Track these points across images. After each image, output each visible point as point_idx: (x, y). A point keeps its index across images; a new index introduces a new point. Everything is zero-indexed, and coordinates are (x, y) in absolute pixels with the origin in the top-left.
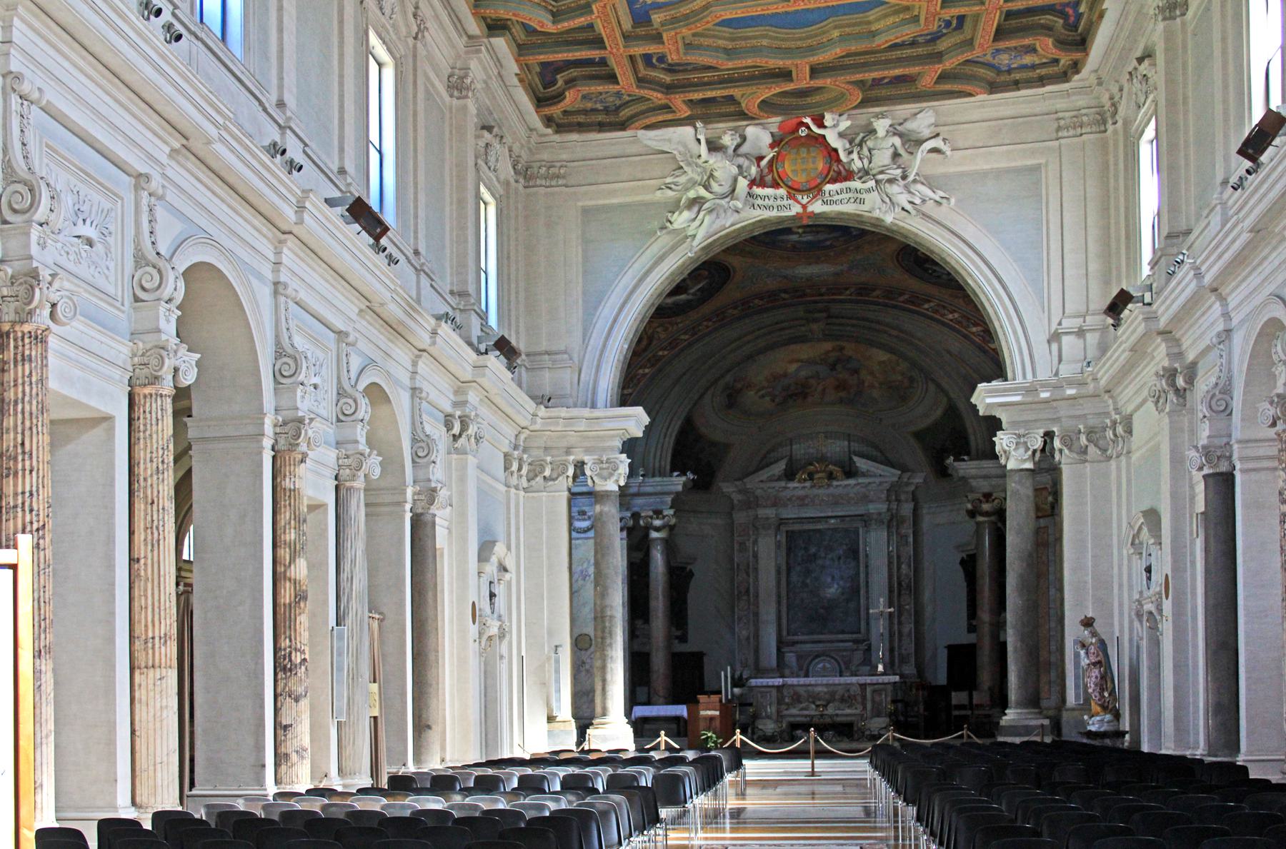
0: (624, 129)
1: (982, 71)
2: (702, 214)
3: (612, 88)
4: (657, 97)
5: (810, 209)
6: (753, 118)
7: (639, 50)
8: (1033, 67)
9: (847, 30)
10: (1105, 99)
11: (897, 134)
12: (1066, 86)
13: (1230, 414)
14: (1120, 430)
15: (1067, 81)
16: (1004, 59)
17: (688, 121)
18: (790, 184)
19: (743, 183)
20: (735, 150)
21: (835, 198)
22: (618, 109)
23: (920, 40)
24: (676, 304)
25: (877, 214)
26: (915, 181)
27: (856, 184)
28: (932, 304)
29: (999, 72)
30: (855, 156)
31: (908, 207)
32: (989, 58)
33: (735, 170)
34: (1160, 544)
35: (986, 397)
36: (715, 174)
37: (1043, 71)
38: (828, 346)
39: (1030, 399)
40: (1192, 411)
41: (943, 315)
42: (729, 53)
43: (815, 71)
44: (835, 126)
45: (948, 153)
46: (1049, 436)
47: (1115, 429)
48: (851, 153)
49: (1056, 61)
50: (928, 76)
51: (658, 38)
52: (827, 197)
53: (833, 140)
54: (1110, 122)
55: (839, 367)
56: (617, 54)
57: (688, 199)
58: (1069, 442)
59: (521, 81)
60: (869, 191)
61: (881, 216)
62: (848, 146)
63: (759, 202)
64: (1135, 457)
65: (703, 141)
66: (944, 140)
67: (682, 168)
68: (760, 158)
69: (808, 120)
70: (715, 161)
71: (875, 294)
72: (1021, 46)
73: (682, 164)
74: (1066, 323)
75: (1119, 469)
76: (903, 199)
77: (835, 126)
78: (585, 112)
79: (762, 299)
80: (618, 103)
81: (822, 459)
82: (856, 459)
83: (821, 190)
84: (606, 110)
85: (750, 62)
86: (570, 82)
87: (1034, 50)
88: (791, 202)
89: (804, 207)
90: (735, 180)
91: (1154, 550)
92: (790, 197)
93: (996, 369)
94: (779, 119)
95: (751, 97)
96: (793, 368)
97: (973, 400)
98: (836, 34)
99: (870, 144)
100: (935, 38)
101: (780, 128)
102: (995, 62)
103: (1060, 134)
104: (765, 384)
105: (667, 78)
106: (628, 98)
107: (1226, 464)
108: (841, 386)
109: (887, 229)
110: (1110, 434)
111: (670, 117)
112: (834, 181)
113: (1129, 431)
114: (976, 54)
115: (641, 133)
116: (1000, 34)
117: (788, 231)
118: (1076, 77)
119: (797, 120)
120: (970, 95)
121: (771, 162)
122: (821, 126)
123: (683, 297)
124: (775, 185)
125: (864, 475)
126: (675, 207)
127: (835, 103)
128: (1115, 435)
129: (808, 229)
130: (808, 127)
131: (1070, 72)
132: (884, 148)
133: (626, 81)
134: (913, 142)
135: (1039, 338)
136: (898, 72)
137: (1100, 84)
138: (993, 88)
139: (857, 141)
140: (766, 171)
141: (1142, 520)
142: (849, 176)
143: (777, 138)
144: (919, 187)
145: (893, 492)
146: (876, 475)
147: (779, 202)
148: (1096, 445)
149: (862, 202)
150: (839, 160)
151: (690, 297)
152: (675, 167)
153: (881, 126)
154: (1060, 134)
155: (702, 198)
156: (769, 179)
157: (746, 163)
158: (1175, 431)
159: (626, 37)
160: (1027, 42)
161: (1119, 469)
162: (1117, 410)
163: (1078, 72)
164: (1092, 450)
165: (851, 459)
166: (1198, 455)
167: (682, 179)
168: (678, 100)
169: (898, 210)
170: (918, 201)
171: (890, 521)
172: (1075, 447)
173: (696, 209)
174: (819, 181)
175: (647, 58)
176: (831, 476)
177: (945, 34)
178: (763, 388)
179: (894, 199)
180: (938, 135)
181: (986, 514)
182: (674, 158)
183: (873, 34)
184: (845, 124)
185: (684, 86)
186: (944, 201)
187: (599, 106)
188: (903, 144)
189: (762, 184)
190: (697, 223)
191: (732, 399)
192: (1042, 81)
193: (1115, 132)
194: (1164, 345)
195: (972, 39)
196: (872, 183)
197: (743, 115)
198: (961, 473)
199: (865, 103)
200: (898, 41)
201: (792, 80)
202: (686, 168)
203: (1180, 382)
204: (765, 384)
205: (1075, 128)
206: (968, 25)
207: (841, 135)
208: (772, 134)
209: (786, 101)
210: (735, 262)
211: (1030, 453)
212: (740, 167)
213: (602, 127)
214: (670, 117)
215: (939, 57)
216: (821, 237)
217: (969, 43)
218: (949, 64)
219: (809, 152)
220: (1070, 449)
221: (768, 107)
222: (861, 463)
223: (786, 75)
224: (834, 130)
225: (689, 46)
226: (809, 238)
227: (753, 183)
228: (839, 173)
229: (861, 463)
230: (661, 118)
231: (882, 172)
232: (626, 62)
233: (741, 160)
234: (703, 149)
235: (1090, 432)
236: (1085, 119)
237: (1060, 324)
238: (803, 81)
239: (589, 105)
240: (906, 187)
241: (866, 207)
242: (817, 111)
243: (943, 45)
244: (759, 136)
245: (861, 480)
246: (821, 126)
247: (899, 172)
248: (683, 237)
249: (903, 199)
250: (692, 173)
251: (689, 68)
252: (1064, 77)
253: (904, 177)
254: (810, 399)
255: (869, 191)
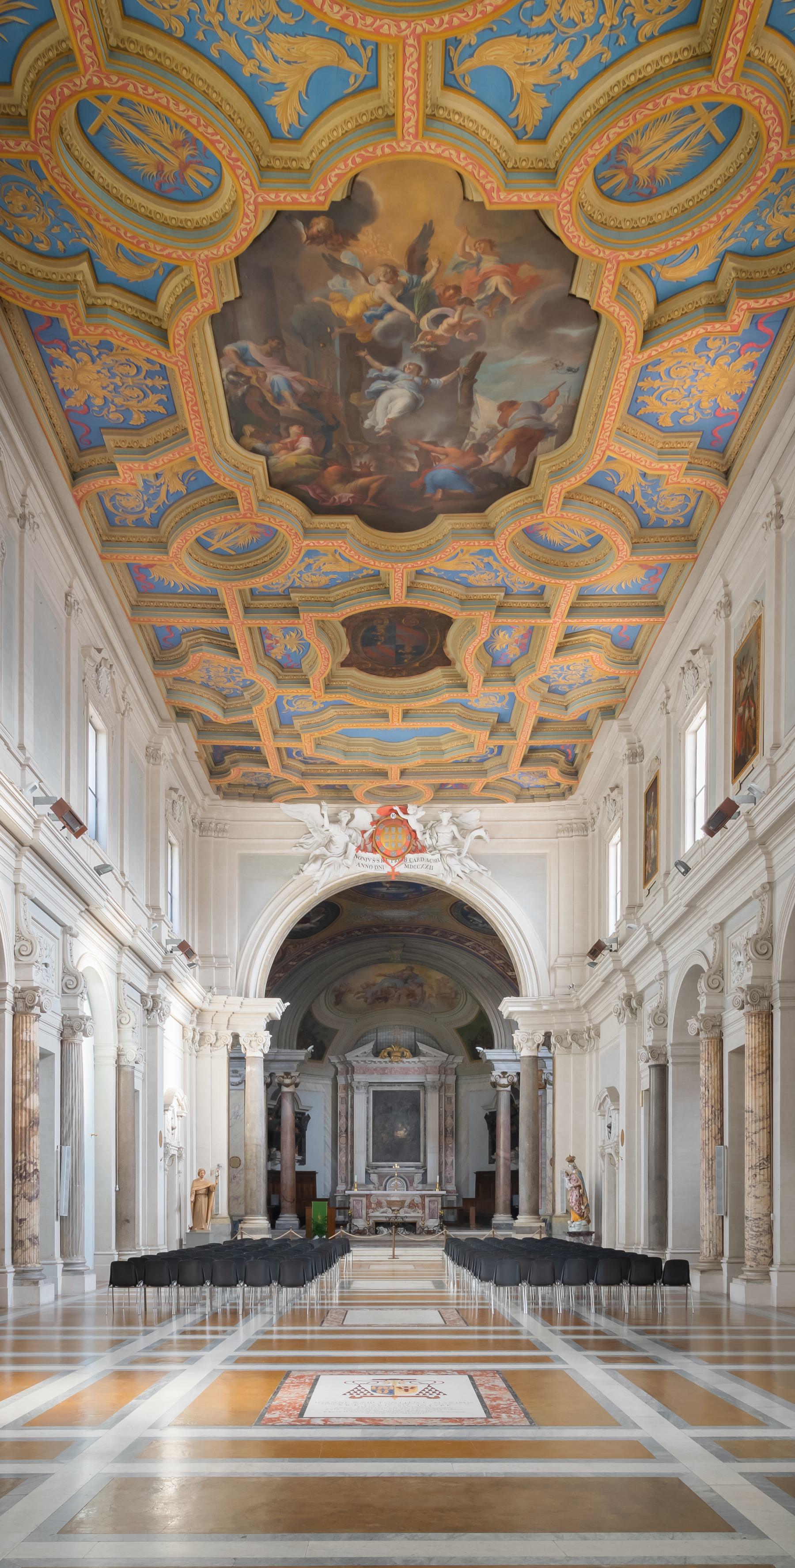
0: (271, 801)
1: (511, 786)
2: (324, 866)
3: (263, 770)
4: (295, 780)
5: (397, 870)
6: (360, 803)
7: (284, 744)
8: (544, 787)
9: (427, 747)
10: (588, 814)
11: (455, 823)
12: (564, 802)
13: (666, 1026)
14: (592, 1033)
15: (565, 799)
16: (526, 780)
17: (316, 800)
18: (384, 851)
19: (352, 848)
20: (347, 824)
21: (414, 864)
22: (267, 786)
23: (473, 760)
24: (302, 930)
25: (441, 877)
26: (466, 857)
27: (427, 855)
28: (471, 943)
29: (522, 788)
30: (427, 836)
31: (461, 874)
32: (516, 778)
33: (348, 839)
34: (618, 1109)
35: (509, 1006)
36: (333, 839)
37: (550, 791)
38: (402, 966)
39: (535, 1009)
40: (640, 1023)
41: (478, 951)
42: (345, 753)
43: (403, 773)
44: (415, 814)
45: (488, 840)
46: (548, 1036)
47: (589, 1034)
48: (424, 834)
49: (558, 785)
50: (478, 784)
51: (298, 737)
52: (408, 863)
53: (414, 825)
54: (590, 829)
55: (409, 981)
56: (268, 745)
57: (314, 856)
58: (560, 1040)
59: (199, 757)
60: (436, 861)
61: (444, 879)
62: (422, 828)
63: (362, 862)
64: (601, 1052)
65: (326, 816)
66: (485, 831)
67: (310, 833)
68: (364, 832)
69: (396, 808)
70: (334, 829)
71: (435, 933)
72: (538, 772)
73: (311, 830)
74: (559, 960)
75: (591, 1059)
76: (457, 869)
77: (415, 814)
78: (244, 786)
79: (359, 930)
80: (267, 781)
81: (397, 1043)
82: (419, 1044)
83: (404, 858)
84: (259, 786)
85: (360, 762)
86: (235, 762)
87: (546, 776)
88: (384, 864)
89: (393, 868)
90: (347, 845)
91: (614, 1114)
92: (384, 860)
93: (513, 987)
94: (379, 805)
95: (361, 786)
96: (379, 980)
97: (500, 1008)
98: (418, 749)
99: (438, 829)
100: (482, 761)
101: (378, 812)
102: (520, 781)
103: (559, 835)
104: (361, 989)
105: (303, 767)
106: (274, 779)
107: (663, 1059)
108: (411, 995)
109: (447, 888)
110: (586, 1036)
111: (303, 795)
112: (413, 852)
113: (598, 1035)
114: (508, 774)
115: (283, 805)
116: (525, 760)
117: (379, 884)
118: (571, 797)
119: (389, 808)
120: (503, 802)
121: (372, 837)
122: (405, 813)
123: (308, 925)
124: (374, 851)
125: (424, 1055)
126: (305, 860)
127: (415, 797)
128: (589, 1037)
129: (393, 885)
130: (397, 813)
131: (567, 793)
132: (445, 834)
133: (274, 768)
134: (464, 831)
135: (542, 968)
136: (457, 780)
137: (585, 803)
138: (518, 798)
139: (429, 826)
140: (367, 841)
141: (606, 1093)
142: (423, 849)
143: (376, 819)
144: (468, 861)
145: (442, 1070)
146: (432, 1056)
147: (376, 863)
148: (577, 1043)
149: (431, 868)
150: (416, 838)
151: (312, 925)
152: (305, 832)
153: (445, 817)
154: (559, 835)
155: (325, 855)
156: (369, 847)
157: (354, 835)
158: (630, 1036)
159: (275, 733)
160: (542, 769)
161: (591, 1059)
162: (590, 1020)
163: (572, 794)
164: (574, 1045)
165: (416, 1045)
166: (644, 1051)
167: (310, 841)
168: (310, 786)
169: (454, 876)
170: (467, 871)
171: (440, 1088)
172: (564, 1043)
173: (319, 862)
174: (403, 851)
175: (289, 751)
176: (403, 1056)
177: (489, 758)
178: (359, 993)
179: (453, 869)
180: (481, 827)
181: (504, 1086)
182: (305, 825)
183: (443, 752)
184: (421, 813)
185: (313, 775)
186: (484, 873)
187: (254, 783)
188: (459, 831)
189: (365, 850)
190: (320, 873)
191: (339, 998)
192: (549, 797)
193: (593, 836)
194: (624, 979)
195: (507, 763)
196: (438, 856)
197: (353, 800)
198: (488, 1058)
199: (435, 800)
200: (459, 759)
201: (388, 779)
202: (314, 834)
203: (634, 1003)
204: (361, 989)
205: (568, 831)
206: (505, 751)
207: (419, 821)
208: (373, 816)
209: (382, 793)
210: (344, 904)
211: (536, 1045)
212: (350, 836)
213: (255, 798)
214: (303, 795)
215: (484, 773)
216: (402, 891)
217: (505, 766)
218: (492, 778)
219: (397, 830)
220: (561, 1045)
221: (371, 795)
222: (423, 1047)
223: (384, 774)
224: (414, 816)
225: (318, 745)
226: (393, 891)
227: (359, 848)
228: (417, 847)
229: (423, 1047)
230: (297, 796)
231: (445, 849)
232: (275, 752)
233: (351, 832)
234: (326, 821)
235: (574, 1034)
236: (575, 826)
237: (556, 961)
238: (394, 780)
239: (247, 781)
240: (460, 861)
241: (433, 872)
242: (403, 803)
243: (487, 765)
244: (364, 816)
245: (422, 1059)
246: (405, 813)
247: (455, 850)
248: (311, 883)
249: (457, 869)
250: (318, 838)
251: (319, 762)
252: (563, 796)
253: (459, 854)
254: (390, 1002)
255: (436, 861)
